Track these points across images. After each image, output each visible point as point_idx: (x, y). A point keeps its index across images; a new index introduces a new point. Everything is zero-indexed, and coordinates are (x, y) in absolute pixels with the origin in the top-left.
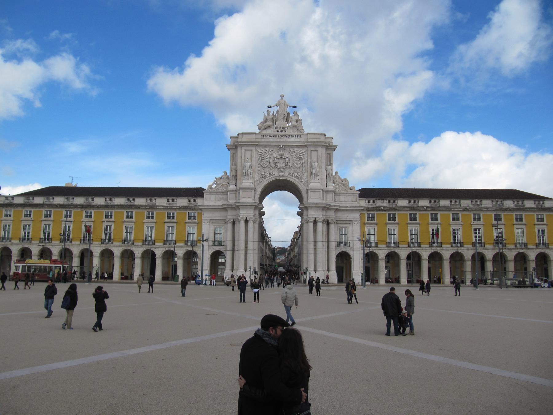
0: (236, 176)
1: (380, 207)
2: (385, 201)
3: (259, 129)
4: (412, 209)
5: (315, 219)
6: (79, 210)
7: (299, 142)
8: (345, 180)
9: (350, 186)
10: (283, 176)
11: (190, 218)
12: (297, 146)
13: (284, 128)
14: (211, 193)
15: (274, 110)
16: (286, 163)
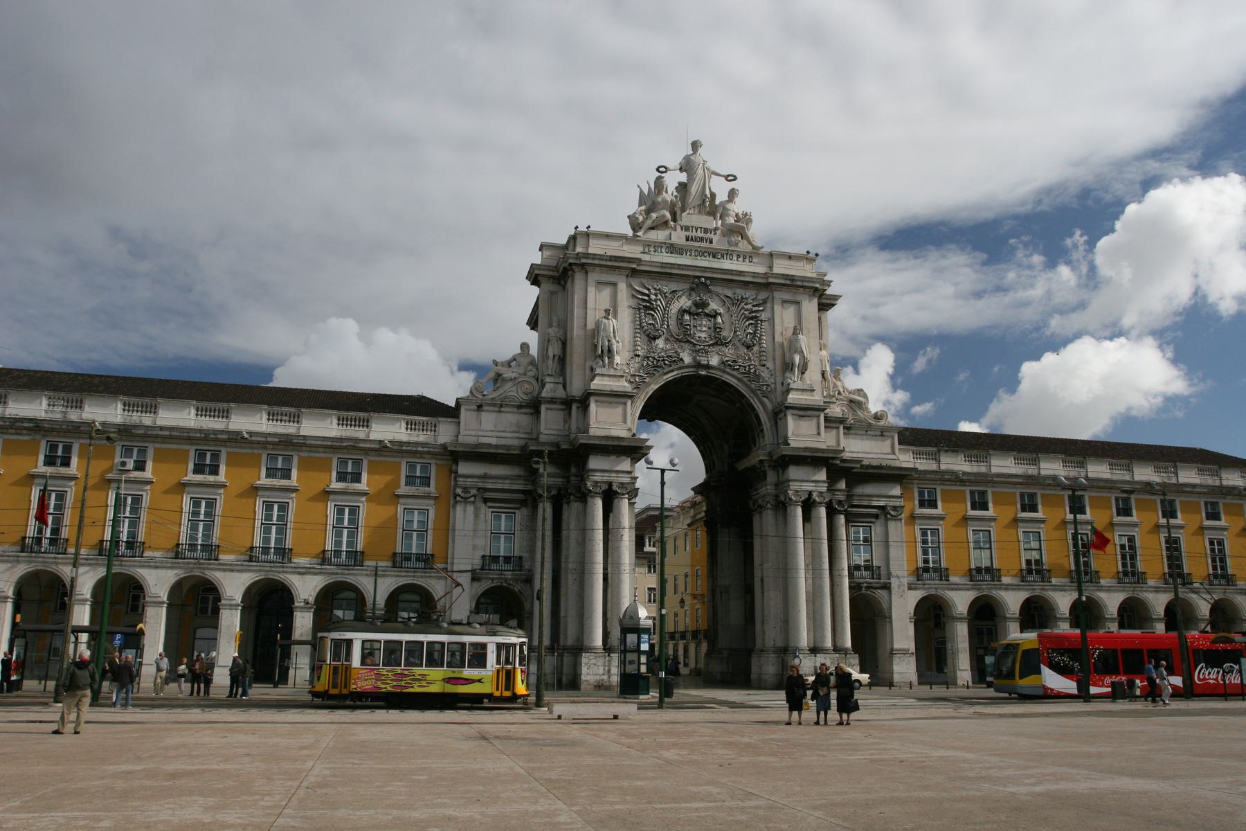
0: (562, 360)
1: (952, 472)
2: (961, 458)
3: (636, 226)
4: (1030, 480)
5: (810, 493)
6: (26, 438)
7: (755, 275)
8: (860, 391)
9: (873, 412)
10: (708, 367)
11: (410, 480)
12: (746, 284)
13: (706, 231)
14: (480, 407)
15: (673, 180)
16: (716, 329)
